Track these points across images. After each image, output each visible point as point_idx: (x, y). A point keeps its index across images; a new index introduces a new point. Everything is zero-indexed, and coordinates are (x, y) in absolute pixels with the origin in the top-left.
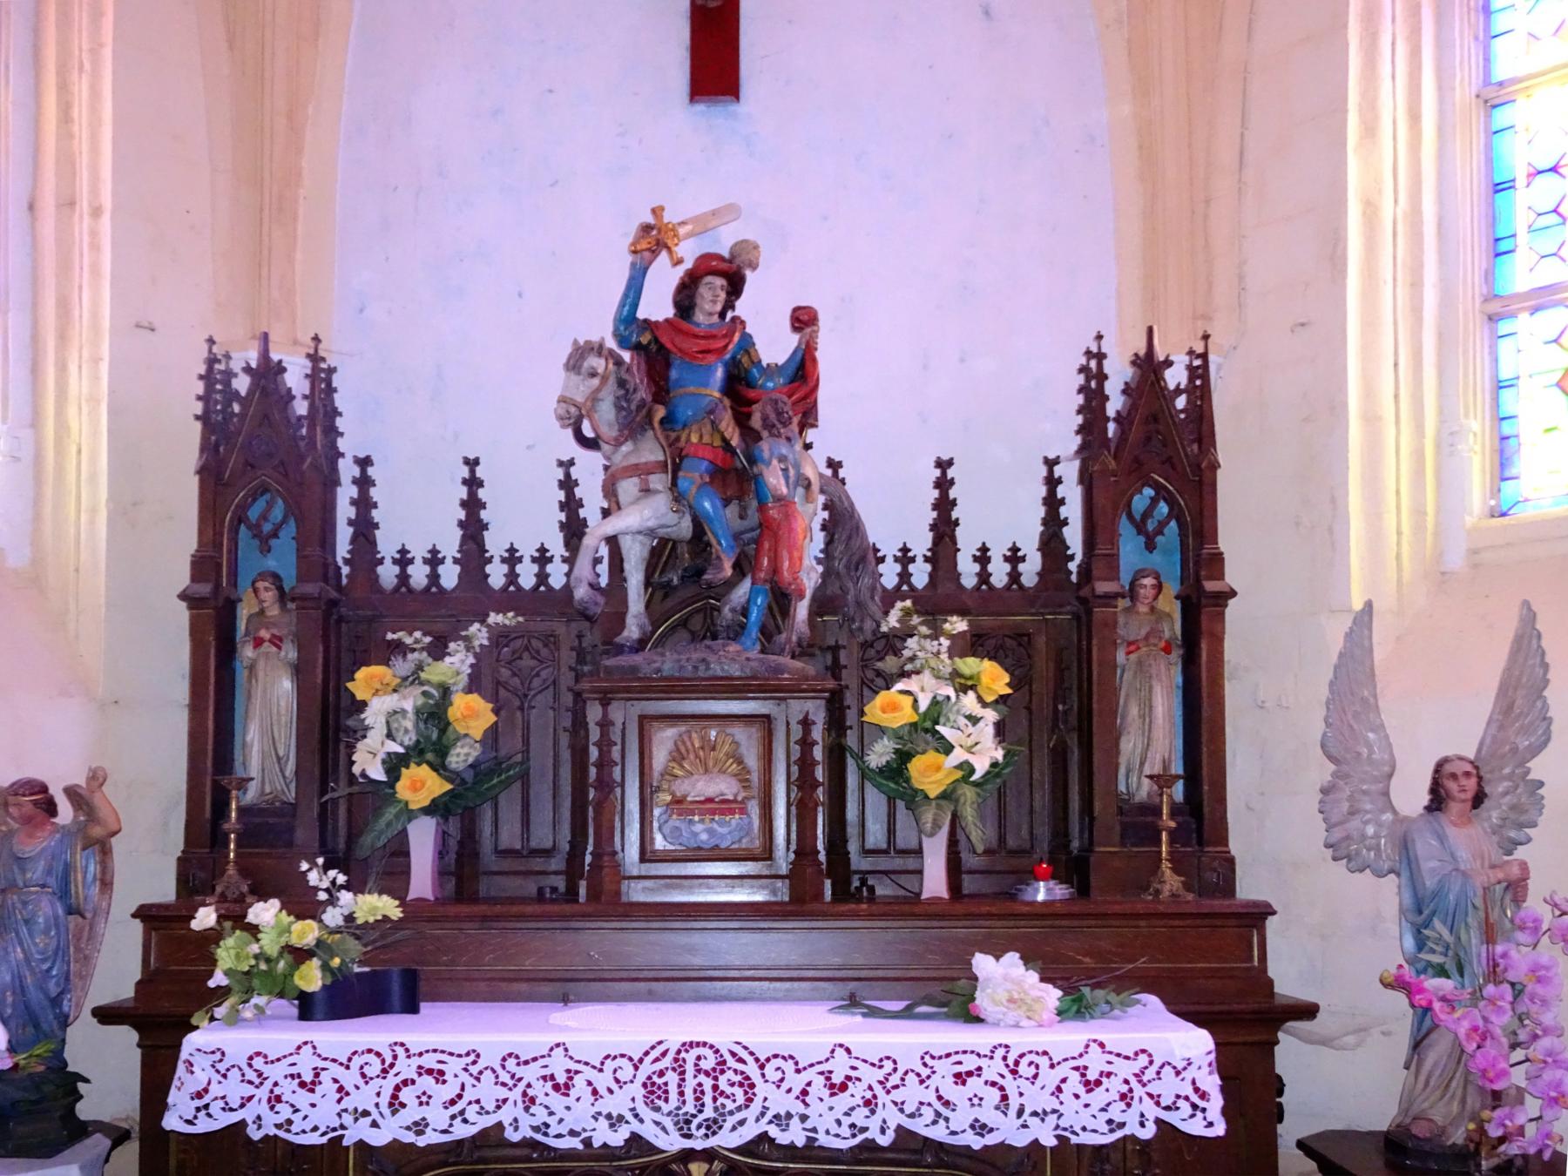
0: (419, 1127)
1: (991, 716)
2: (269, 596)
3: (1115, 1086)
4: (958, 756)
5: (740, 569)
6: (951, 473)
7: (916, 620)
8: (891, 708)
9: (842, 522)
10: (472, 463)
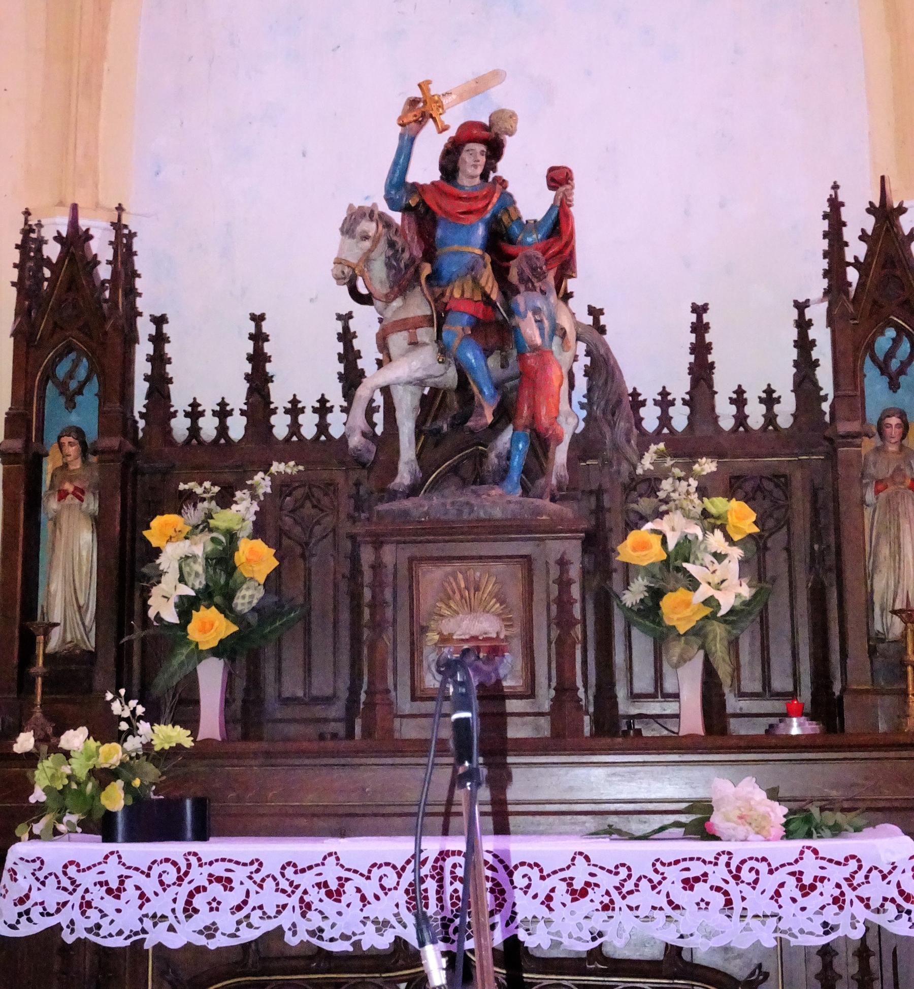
0: (210, 931)
1: (736, 553)
2: (73, 450)
3: (828, 889)
4: (704, 591)
5: (505, 413)
6: (706, 318)
7: (669, 462)
8: (640, 548)
9: (602, 368)
10: (258, 319)
